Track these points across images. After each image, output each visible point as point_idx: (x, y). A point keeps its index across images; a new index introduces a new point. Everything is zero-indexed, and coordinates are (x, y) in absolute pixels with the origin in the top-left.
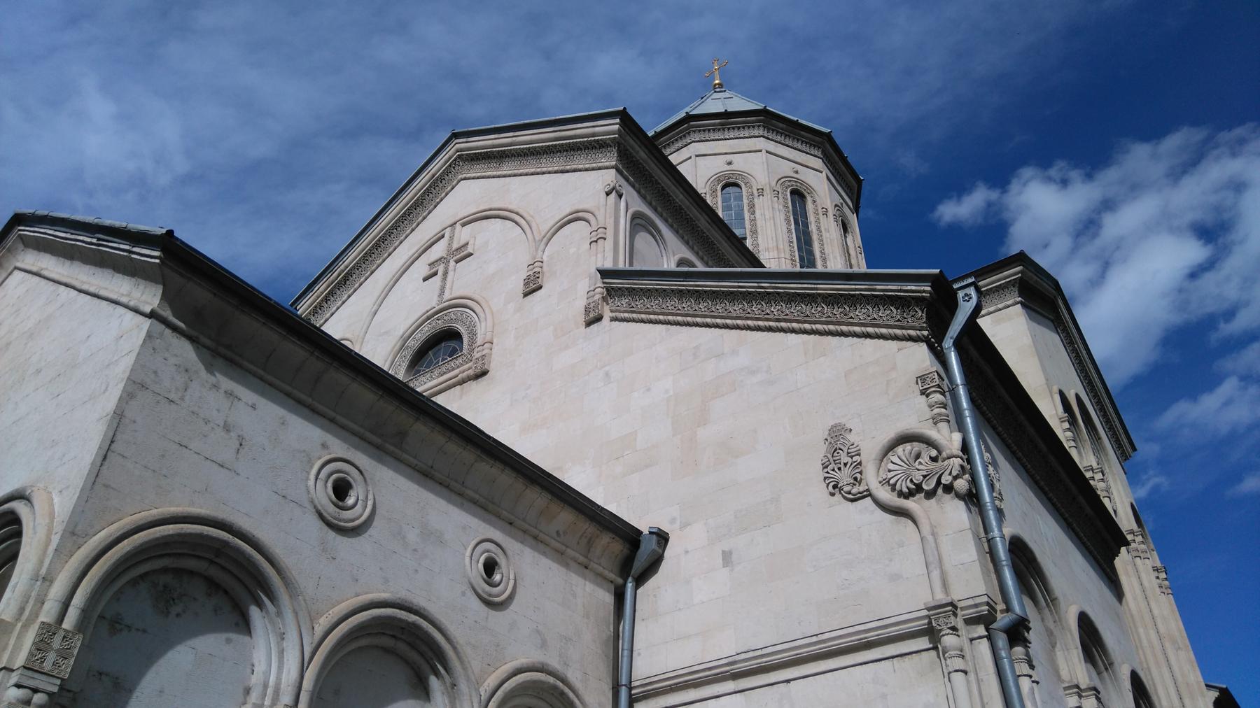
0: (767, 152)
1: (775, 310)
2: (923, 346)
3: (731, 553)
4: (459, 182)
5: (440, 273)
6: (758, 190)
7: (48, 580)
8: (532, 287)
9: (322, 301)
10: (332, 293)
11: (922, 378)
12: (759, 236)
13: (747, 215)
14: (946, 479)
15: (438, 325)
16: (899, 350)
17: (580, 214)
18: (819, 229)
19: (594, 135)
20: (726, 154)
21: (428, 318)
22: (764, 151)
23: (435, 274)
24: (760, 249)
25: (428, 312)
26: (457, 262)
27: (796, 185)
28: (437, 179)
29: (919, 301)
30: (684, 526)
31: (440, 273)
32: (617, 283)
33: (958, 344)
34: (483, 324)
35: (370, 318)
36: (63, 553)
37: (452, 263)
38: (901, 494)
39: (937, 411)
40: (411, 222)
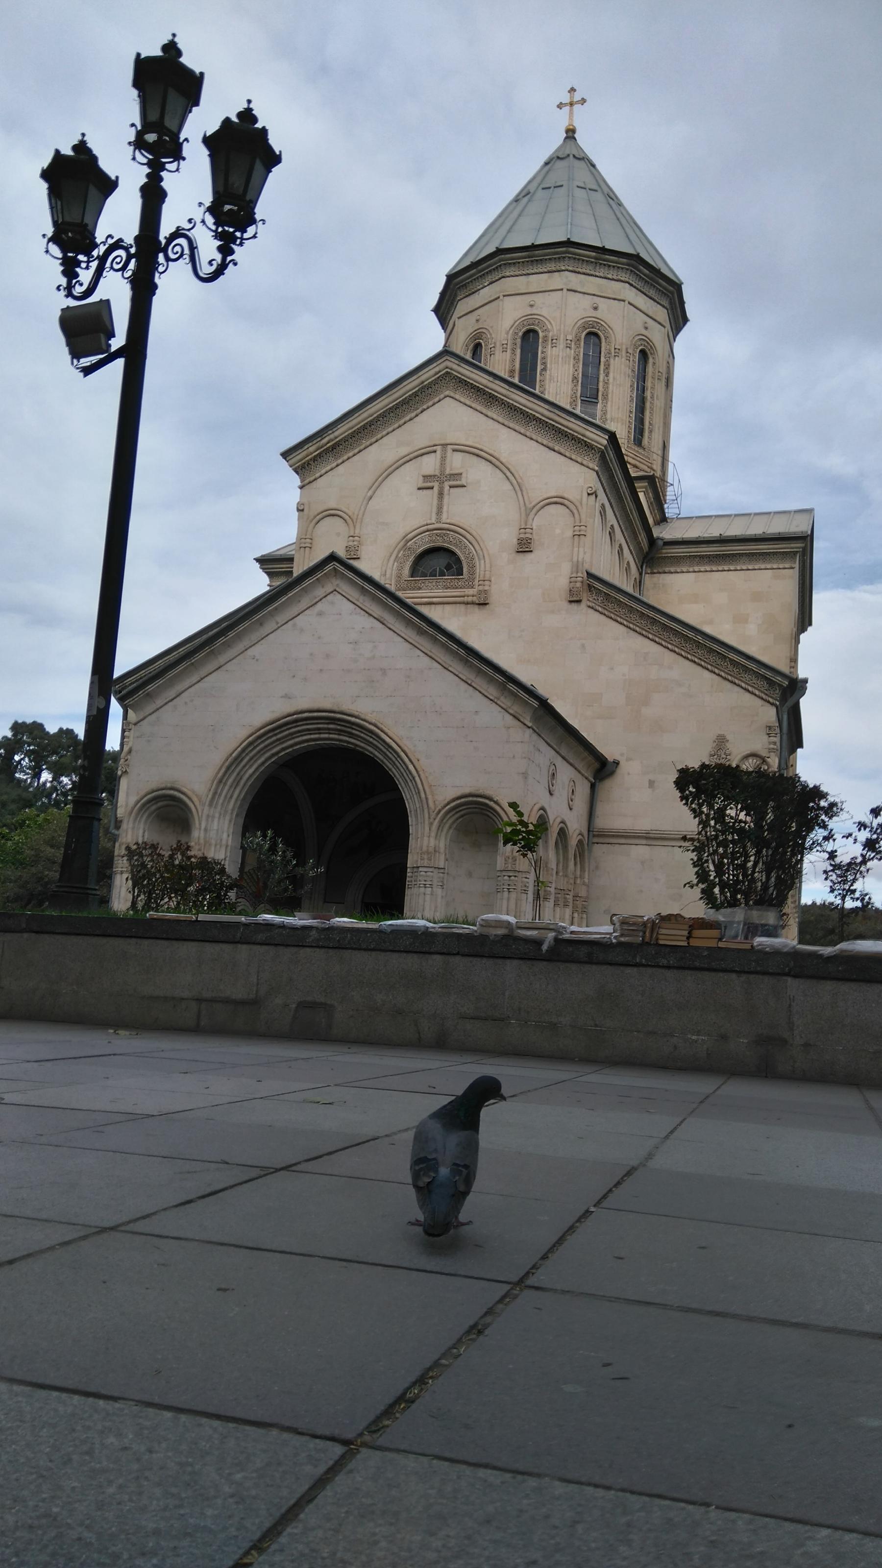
0: (629, 303)
2: (775, 709)
3: (654, 782)
4: (445, 397)
5: (436, 489)
6: (615, 349)
8: (524, 547)
9: (311, 459)
10: (320, 455)
11: (770, 728)
12: (609, 403)
15: (439, 543)
16: (762, 706)
17: (566, 502)
18: (652, 397)
19: (583, 435)
20: (594, 295)
21: (428, 531)
22: (627, 302)
23: (432, 488)
24: (608, 416)
25: (427, 525)
26: (450, 487)
27: (645, 345)
28: (425, 386)
29: (780, 686)
30: (628, 759)
32: (598, 585)
34: (482, 562)
35: (365, 502)
37: (447, 488)
39: (772, 746)
40: (399, 418)
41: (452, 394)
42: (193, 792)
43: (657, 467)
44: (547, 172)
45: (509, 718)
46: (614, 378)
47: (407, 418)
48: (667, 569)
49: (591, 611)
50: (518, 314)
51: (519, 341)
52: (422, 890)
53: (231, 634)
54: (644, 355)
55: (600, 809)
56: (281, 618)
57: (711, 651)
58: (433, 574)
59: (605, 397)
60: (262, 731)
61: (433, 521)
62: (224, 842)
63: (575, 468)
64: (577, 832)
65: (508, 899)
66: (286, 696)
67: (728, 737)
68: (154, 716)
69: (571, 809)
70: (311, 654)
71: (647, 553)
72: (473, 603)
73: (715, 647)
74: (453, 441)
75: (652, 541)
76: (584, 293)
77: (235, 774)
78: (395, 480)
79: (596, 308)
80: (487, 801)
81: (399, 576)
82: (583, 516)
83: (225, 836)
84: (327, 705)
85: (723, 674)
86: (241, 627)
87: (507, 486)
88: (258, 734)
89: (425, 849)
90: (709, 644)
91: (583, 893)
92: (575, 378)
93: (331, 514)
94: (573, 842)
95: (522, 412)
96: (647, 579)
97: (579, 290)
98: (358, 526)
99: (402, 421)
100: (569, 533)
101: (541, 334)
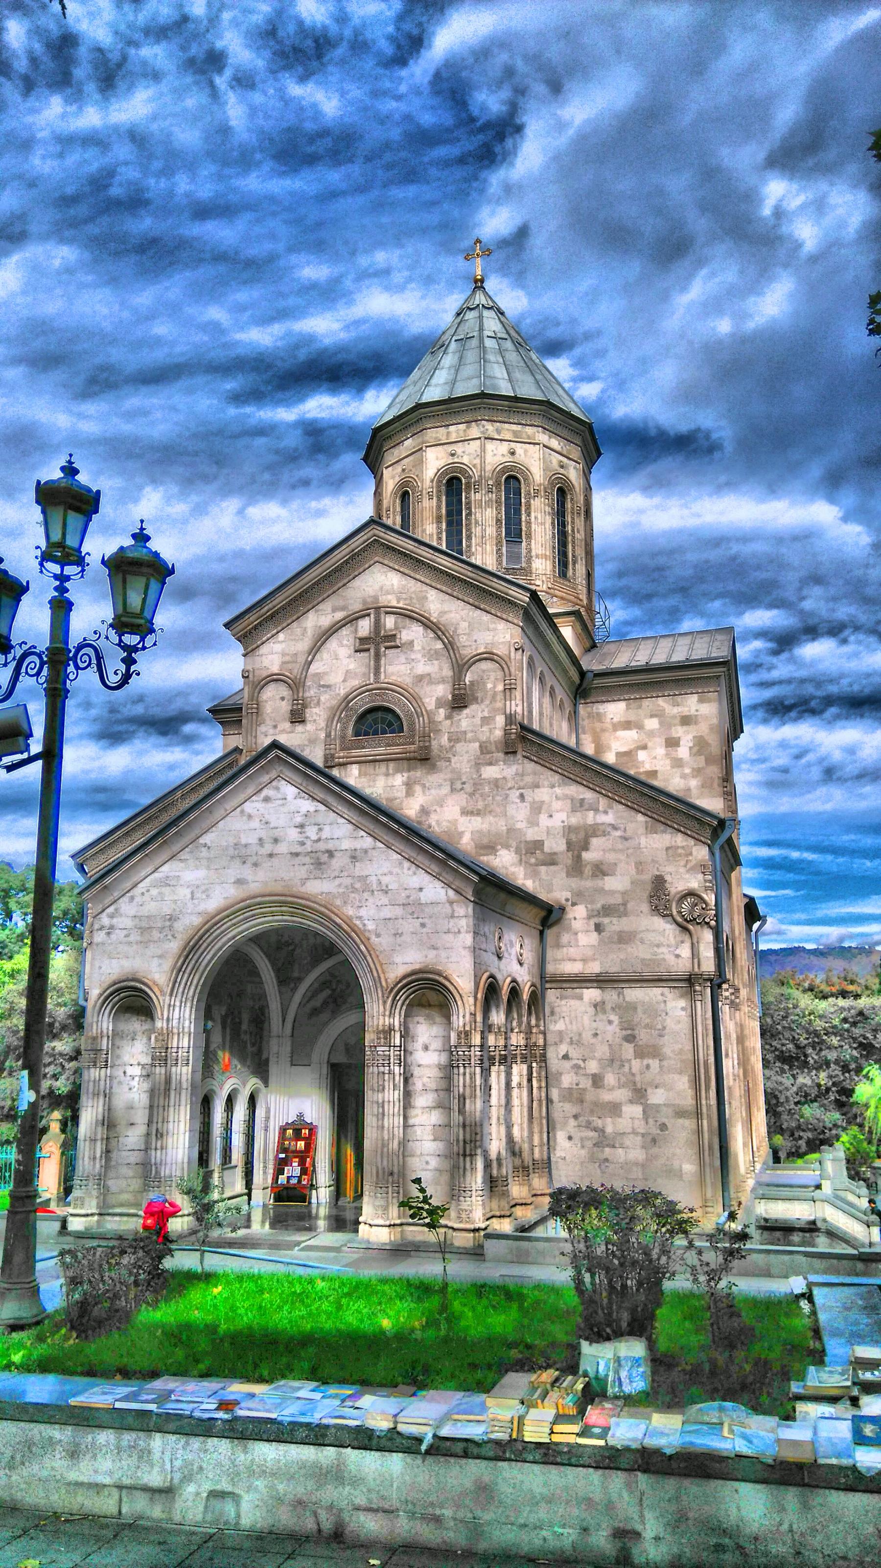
0: (544, 446)
1: (632, 796)
5: (372, 651)
7: (475, 1015)
10: (260, 624)
13: (523, 518)
14: (707, 920)
18: (573, 531)
23: (368, 650)
24: (533, 553)
26: (386, 648)
30: (574, 904)
31: (372, 651)
32: (530, 736)
33: (722, 847)
36: (475, 1005)
38: (686, 920)
40: (332, 584)
41: (381, 560)
42: (154, 983)
43: (584, 597)
44: (459, 324)
45: (451, 893)
46: (536, 518)
47: (341, 584)
48: (599, 699)
49: (526, 761)
50: (442, 463)
51: (443, 488)
52: (381, 1069)
53: (182, 824)
54: (562, 492)
55: (550, 954)
56: (230, 805)
57: (643, 794)
58: (376, 733)
59: (529, 536)
60: (217, 918)
61: (372, 681)
62: (186, 1030)
63: (501, 626)
64: (529, 984)
65: (464, 1074)
66: (239, 882)
67: (668, 878)
68: (111, 910)
69: (521, 964)
70: (260, 839)
71: (580, 685)
72: (415, 759)
73: (646, 790)
74: (386, 604)
75: (582, 674)
76: (501, 440)
77: (193, 962)
78: (333, 644)
79: (513, 454)
80: (437, 978)
81: (343, 737)
82: (513, 670)
83: (187, 1023)
84: (278, 888)
85: (655, 816)
86: (192, 816)
87: (439, 645)
88: (213, 921)
89: (381, 1028)
90: (639, 788)
91: (541, 1042)
92: (498, 521)
93: (274, 679)
94: (525, 996)
95: (448, 575)
96: (582, 710)
97: (497, 437)
98: (301, 690)
99: (335, 588)
100: (500, 687)
101: (463, 481)
